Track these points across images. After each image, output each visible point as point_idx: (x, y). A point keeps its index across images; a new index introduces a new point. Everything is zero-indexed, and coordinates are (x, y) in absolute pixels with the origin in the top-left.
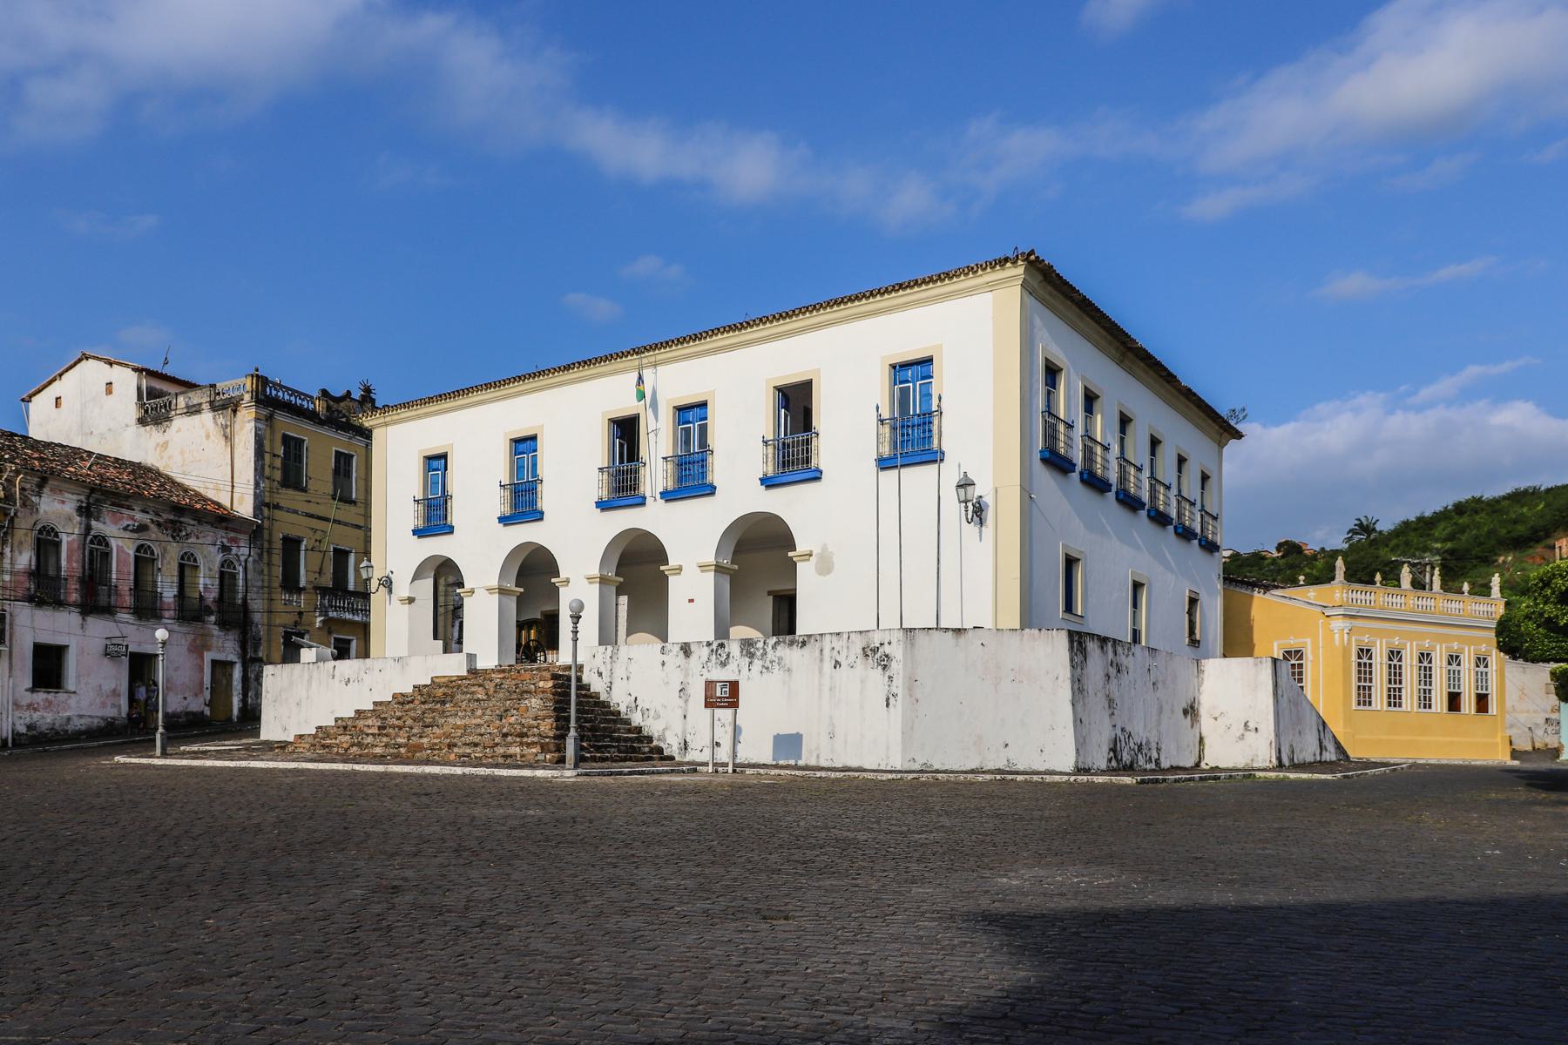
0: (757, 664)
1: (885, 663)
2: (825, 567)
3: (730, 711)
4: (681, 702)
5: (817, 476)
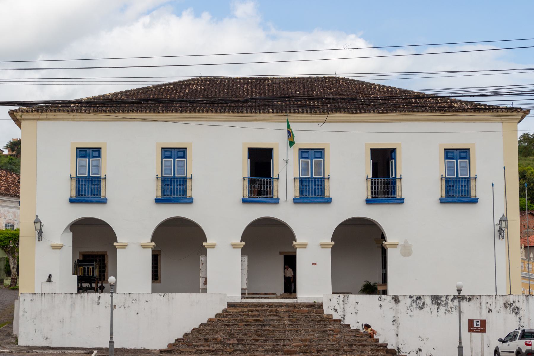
0: (442, 309)
1: (516, 310)
2: (407, 251)
3: (480, 334)
4: (394, 327)
5: (401, 201)
